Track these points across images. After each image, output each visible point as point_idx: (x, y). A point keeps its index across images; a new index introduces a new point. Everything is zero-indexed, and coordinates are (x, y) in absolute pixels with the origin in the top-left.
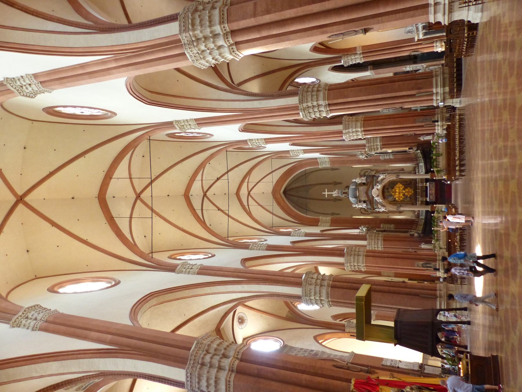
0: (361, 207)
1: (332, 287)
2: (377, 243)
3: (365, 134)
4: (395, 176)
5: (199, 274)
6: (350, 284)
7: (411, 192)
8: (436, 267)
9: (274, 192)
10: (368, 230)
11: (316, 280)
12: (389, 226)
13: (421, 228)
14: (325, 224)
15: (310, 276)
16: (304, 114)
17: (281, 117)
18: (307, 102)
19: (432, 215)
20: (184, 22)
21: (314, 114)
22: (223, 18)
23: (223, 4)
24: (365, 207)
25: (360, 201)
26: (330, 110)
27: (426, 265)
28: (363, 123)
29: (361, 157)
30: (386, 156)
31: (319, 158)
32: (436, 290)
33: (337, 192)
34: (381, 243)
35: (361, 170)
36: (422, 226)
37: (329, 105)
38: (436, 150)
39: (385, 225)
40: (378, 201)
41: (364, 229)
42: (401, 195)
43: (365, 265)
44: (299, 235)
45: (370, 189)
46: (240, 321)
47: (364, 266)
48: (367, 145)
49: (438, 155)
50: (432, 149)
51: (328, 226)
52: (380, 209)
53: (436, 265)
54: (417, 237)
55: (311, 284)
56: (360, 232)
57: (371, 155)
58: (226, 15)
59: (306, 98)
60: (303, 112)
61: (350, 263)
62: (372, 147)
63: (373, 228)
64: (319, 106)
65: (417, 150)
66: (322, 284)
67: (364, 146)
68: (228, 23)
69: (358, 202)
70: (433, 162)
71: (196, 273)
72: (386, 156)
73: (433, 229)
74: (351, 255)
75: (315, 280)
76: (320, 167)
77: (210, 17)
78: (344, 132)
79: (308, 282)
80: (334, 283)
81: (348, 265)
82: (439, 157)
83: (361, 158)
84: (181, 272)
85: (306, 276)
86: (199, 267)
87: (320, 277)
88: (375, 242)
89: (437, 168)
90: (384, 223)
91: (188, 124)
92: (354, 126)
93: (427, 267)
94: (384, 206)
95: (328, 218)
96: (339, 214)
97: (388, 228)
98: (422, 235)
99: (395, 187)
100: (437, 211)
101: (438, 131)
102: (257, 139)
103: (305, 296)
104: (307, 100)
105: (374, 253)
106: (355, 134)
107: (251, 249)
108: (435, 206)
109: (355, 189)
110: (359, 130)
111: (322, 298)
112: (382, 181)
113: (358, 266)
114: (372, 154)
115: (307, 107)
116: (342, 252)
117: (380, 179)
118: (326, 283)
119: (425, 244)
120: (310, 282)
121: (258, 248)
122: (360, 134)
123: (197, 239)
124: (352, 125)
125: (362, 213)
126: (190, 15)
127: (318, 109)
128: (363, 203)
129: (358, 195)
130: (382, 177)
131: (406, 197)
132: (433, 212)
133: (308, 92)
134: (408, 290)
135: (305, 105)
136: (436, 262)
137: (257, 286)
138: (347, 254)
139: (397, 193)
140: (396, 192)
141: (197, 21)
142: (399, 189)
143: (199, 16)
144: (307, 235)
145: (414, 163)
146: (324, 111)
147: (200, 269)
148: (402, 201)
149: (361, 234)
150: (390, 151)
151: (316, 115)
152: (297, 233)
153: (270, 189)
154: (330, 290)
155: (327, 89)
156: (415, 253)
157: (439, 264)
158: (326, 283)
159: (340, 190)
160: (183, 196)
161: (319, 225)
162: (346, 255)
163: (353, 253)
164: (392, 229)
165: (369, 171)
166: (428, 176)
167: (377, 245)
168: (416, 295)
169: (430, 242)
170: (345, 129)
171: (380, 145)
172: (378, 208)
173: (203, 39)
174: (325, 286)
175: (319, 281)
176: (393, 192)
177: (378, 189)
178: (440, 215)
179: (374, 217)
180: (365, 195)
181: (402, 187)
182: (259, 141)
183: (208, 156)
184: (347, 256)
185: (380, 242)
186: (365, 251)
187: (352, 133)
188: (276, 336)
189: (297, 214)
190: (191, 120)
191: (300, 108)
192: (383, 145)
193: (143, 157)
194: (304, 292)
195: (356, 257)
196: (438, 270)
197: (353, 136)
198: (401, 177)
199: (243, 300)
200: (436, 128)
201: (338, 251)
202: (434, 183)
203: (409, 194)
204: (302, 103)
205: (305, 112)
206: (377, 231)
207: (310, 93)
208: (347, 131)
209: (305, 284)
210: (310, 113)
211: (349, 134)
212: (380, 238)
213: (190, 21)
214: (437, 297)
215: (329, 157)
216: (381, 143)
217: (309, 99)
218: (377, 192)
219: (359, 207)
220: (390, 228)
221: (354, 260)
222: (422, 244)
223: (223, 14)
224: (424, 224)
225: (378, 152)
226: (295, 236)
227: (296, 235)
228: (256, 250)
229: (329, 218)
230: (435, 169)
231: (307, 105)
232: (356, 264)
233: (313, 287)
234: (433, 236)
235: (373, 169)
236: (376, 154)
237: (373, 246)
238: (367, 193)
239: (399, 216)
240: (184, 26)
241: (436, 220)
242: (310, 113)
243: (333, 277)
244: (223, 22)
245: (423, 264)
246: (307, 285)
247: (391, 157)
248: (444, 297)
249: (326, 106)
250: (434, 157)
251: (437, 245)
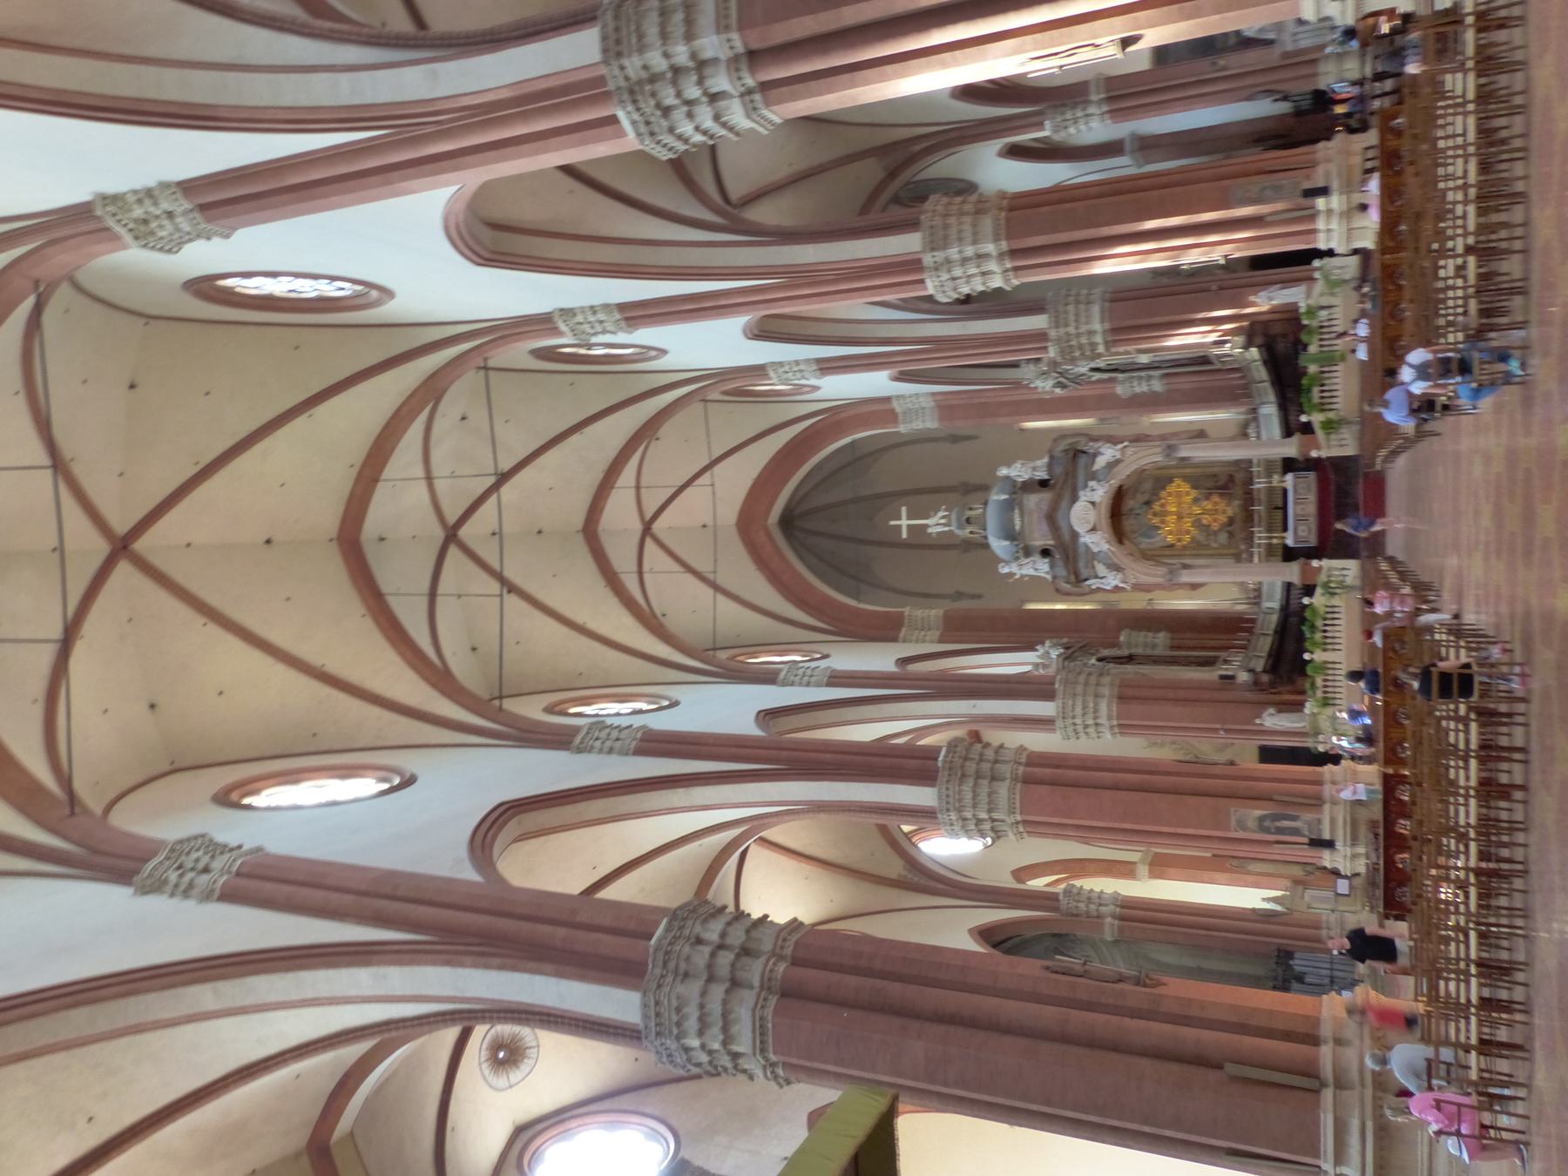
0: (1032, 572)
1: (785, 994)
2: (1096, 711)
3: (1016, 269)
4: (1159, 450)
5: (230, 896)
6: (870, 982)
7: (1224, 512)
8: (1320, 830)
9: (747, 522)
10: (1067, 658)
11: (713, 955)
12: (1149, 640)
13: (1265, 644)
14: (923, 633)
15: (687, 932)
16: (636, 116)
17: (540, 143)
18: (642, 49)
19: (1306, 601)
21: (690, 115)
24: (1047, 573)
25: (1028, 552)
26: (765, 87)
27: (1278, 824)
29: (1039, 383)
30: (1135, 384)
31: (898, 397)
32: (1314, 1040)
33: (943, 517)
34: (1110, 709)
35: (1055, 440)
36: (1269, 640)
37: (754, 57)
38: (1321, 340)
39: (1134, 634)
40: (1095, 550)
41: (1054, 653)
42: (1187, 524)
43: (1019, 818)
44: (806, 679)
45: (1064, 504)
46: (501, 1055)
47: (1017, 823)
48: (1053, 333)
49: (1329, 359)
50: (1304, 338)
51: (932, 642)
52: (1103, 581)
53: (1319, 821)
54: (1245, 687)
55: (686, 975)
56: (1036, 665)
57: (1077, 380)
60: (630, 108)
61: (959, 810)
62: (1073, 343)
63: (1085, 649)
64: (702, 66)
65: (1246, 347)
66: (741, 975)
67: (1040, 336)
69: (1021, 554)
70: (1309, 391)
71: (217, 894)
72: (1135, 384)
73: (1306, 656)
74: (963, 776)
75: (707, 950)
76: (902, 429)
78: (928, 259)
79: (672, 965)
80: (801, 973)
81: (953, 818)
82: (1335, 368)
83: (1040, 390)
84: (156, 886)
85: (667, 930)
86: (239, 862)
87: (737, 936)
88: (1085, 707)
89: (1323, 410)
90: (1132, 629)
91: (158, 212)
92: (968, 235)
93: (1280, 831)
94: (1116, 568)
95: (933, 612)
96: (979, 597)
97: (1146, 645)
98: (1265, 678)
99: (1163, 494)
100: (1326, 586)
101: (1328, 240)
102: (592, 307)
103: (658, 1034)
104: (641, 37)
105: (1058, 767)
106: (973, 271)
107: (579, 751)
108: (1315, 563)
109: (1009, 506)
110: (990, 248)
111: (736, 1048)
112: (1109, 473)
113: (993, 820)
114: (1083, 375)
115: (644, 75)
116: (930, 763)
117: (1100, 462)
118: (754, 971)
119: (1280, 711)
120: (683, 966)
121: (608, 744)
122: (993, 266)
123: (375, 711)
124: (960, 232)
125: (1057, 590)
127: (700, 82)
128: (1037, 557)
129: (1018, 527)
130: (1108, 453)
131: (1205, 529)
132: (1309, 590)
134: (1159, 1032)
135: (633, 65)
136: (1321, 812)
137: (445, 971)
138: (946, 773)
139: (1168, 519)
140: (1164, 514)
142: (1179, 499)
144: (836, 679)
145: (1242, 404)
146: (730, 96)
147: (238, 874)
148: (1184, 547)
149: (1042, 672)
150: (1144, 359)
151: (698, 120)
152: (800, 672)
153: (729, 513)
154: (775, 1012)
156: (1229, 770)
157: (1333, 821)
158: (754, 971)
159: (956, 510)
160: (334, 543)
161: (902, 635)
162: (943, 776)
163: (971, 767)
164: (1159, 651)
165: (1083, 440)
166: (1291, 449)
167: (1095, 718)
168: (1202, 1061)
169: (1297, 707)
170: (933, 249)
171: (1105, 332)
172: (1096, 577)
174: (751, 987)
175: (725, 958)
176: (1155, 514)
177: (1093, 503)
178: (1336, 601)
179: (1098, 607)
180: (1045, 527)
181: (1188, 494)
182: (601, 316)
183: (418, 383)
184: (948, 781)
185: (1103, 707)
186: (1023, 760)
187: (962, 265)
188: (657, 1113)
189: (827, 600)
190: (164, 186)
191: (611, 86)
192: (1114, 331)
193: (132, 387)
194: (653, 1014)
195: (985, 782)
196: (1329, 844)
197: (968, 276)
198: (1183, 454)
199: (394, 1034)
200: (1321, 224)
201: (913, 758)
202: (1312, 476)
203: (1215, 521)
204: (619, 55)
205: (642, 105)
206: (1100, 660)
208: (940, 255)
209: (658, 971)
210: (667, 111)
211: (949, 271)
212: (1106, 691)
214: (1324, 1085)
215: (933, 394)
216: (1107, 326)
217: (652, 31)
218: (1092, 516)
219: (1024, 572)
220: (1154, 646)
221: (974, 797)
222: (1264, 715)
224: (1276, 632)
225: (1100, 363)
226: (792, 684)
227: (797, 679)
228: (601, 751)
229: (935, 613)
230: (1316, 418)
231: (645, 67)
232: (984, 815)
233: (693, 989)
234: (1308, 685)
235: (1096, 433)
236: (1097, 376)
237: (1078, 721)
238: (1051, 518)
239: (1191, 599)
241: (1319, 623)
242: (667, 111)
243: (795, 937)
245: (1261, 819)
246: (670, 979)
247: (1158, 386)
248: (1363, 1085)
249: (734, 62)
250: (1313, 369)
251: (1324, 724)
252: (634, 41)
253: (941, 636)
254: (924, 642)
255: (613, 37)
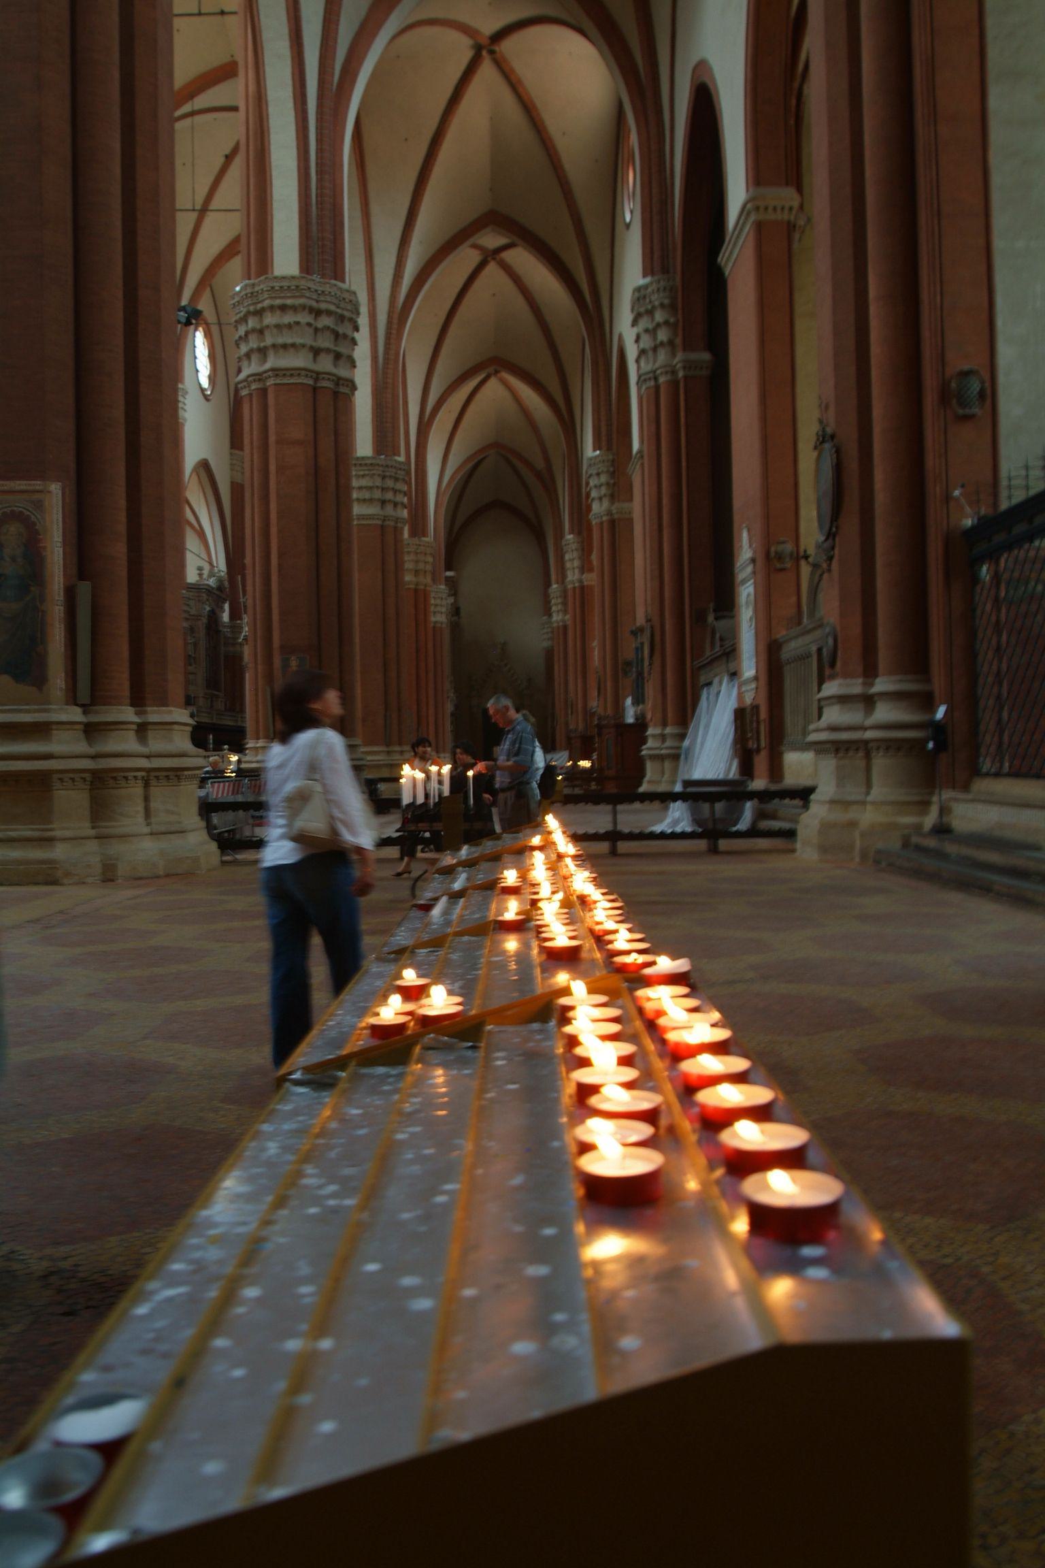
20: (289, 287)
22: (284, 375)
23: (318, 373)
28: (409, 589)
58: (292, 381)
59: (368, 475)
68: (275, 384)
77: (293, 345)
104: (363, 476)
126: (302, 301)
133: (384, 477)
141: (288, 318)
143: (298, 323)
155: (387, 523)
173: (258, 327)
207: (378, 482)
213: (289, 302)
223: (292, 375)
240: (281, 287)
244: (277, 375)
252: (362, 473)
253: (237, 483)
254: (232, 470)
255: (363, 462)
